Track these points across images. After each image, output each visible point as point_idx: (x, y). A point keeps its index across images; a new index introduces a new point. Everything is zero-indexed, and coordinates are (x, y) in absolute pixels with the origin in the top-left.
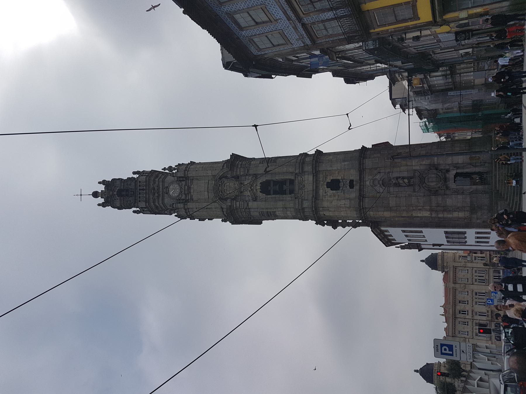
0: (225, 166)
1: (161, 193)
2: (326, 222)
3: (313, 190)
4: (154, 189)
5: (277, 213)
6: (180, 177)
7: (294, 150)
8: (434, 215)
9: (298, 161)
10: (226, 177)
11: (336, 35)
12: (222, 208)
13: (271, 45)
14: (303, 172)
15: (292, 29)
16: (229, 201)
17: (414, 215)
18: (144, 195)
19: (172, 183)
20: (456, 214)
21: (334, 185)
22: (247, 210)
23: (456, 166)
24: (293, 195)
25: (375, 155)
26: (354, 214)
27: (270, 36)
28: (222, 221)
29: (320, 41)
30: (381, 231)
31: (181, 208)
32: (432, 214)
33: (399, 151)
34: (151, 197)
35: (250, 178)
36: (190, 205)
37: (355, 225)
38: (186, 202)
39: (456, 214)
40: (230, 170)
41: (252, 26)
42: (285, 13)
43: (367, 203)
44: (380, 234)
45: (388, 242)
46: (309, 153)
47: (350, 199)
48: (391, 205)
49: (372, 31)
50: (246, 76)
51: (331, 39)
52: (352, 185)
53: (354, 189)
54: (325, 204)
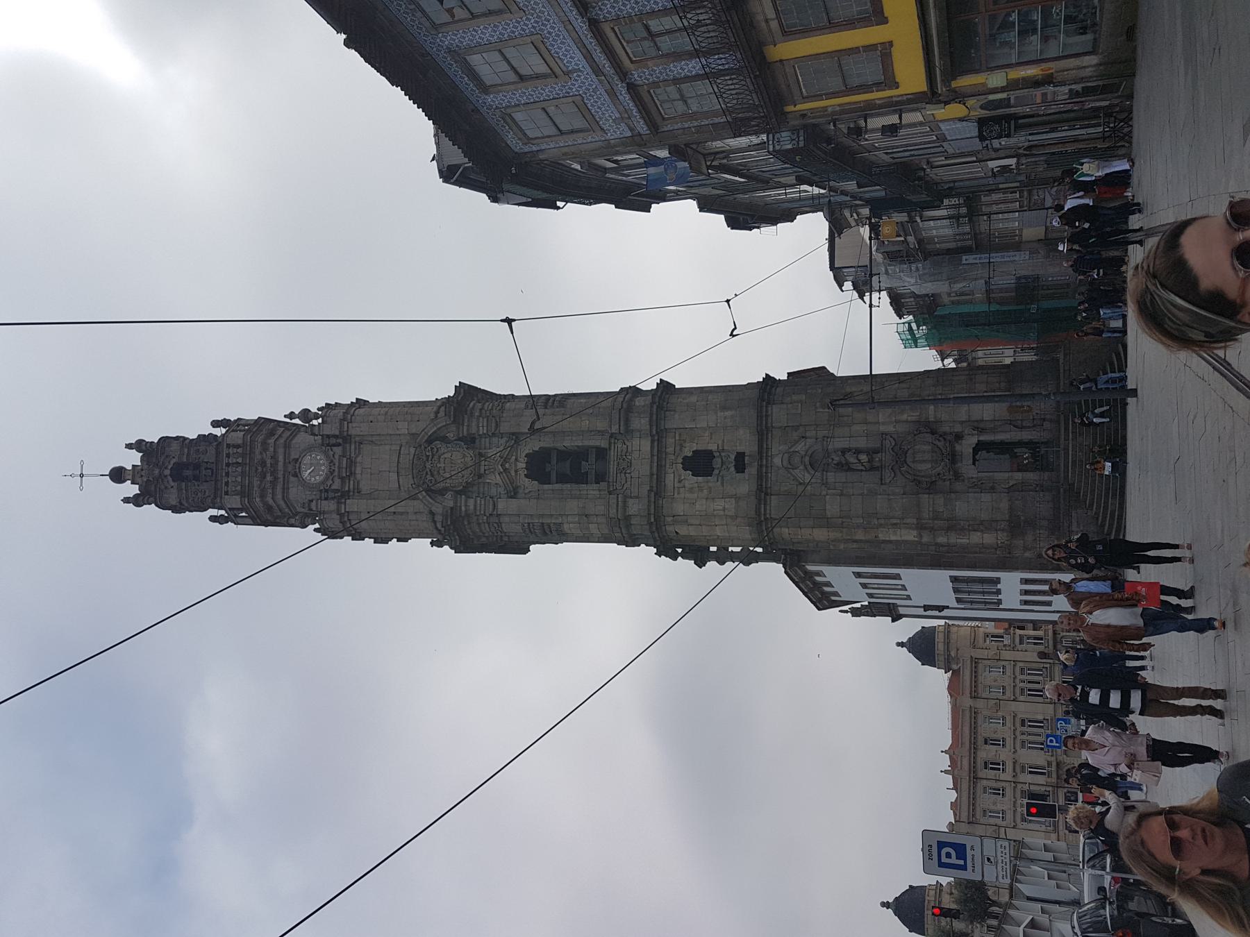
0: (442, 413)
1: (280, 475)
2: (680, 550)
3: (652, 474)
4: (263, 463)
5: (566, 526)
6: (328, 436)
7: (607, 378)
8: (925, 539)
9: (618, 405)
11: (706, 115)
12: (432, 513)
13: (553, 131)
14: (628, 432)
16: (449, 495)
17: (881, 537)
18: (239, 479)
19: (310, 449)
20: (976, 538)
21: (701, 464)
22: (492, 520)
23: (979, 427)
24: (604, 485)
25: (795, 397)
26: (746, 533)
27: (551, 110)
28: (432, 544)
29: (669, 127)
30: (806, 572)
31: (330, 512)
32: (921, 536)
33: (848, 390)
34: (256, 483)
35: (503, 441)
36: (352, 505)
38: (343, 496)
39: (976, 538)
40: (454, 422)
41: (509, 84)
42: (588, 56)
43: (775, 506)
44: (803, 580)
45: (822, 598)
46: (644, 387)
47: (737, 498)
48: (829, 514)
49: (790, 108)
50: (494, 199)
53: (746, 475)
54: (680, 508)
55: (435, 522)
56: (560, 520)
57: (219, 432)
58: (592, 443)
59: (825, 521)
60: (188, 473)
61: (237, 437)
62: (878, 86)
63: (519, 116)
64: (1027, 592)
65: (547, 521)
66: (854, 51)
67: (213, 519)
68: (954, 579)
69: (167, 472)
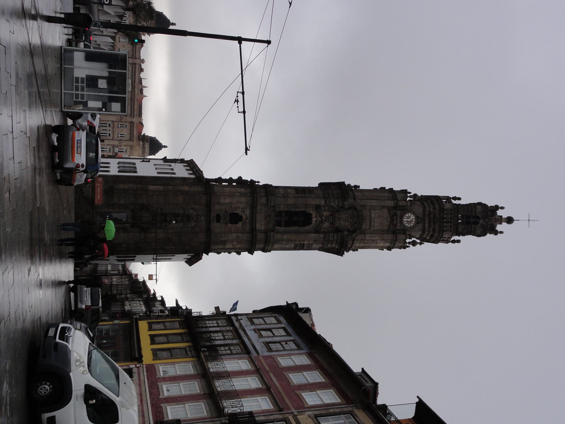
1: (427, 218)
3: (256, 214)
4: (434, 223)
5: (294, 192)
7: (277, 257)
10: (349, 231)
12: (355, 199)
14: (266, 232)
16: (347, 206)
17: (162, 187)
18: (445, 216)
21: (235, 218)
24: (277, 210)
28: (359, 187)
35: (322, 230)
36: (391, 203)
37: (220, 180)
38: (396, 207)
39: (126, 187)
45: (191, 165)
54: (243, 199)
55: (354, 195)
56: (297, 195)
57: (456, 238)
58: (283, 228)
62: (154, 323)
64: (108, 167)
67: (459, 199)
68: (136, 172)
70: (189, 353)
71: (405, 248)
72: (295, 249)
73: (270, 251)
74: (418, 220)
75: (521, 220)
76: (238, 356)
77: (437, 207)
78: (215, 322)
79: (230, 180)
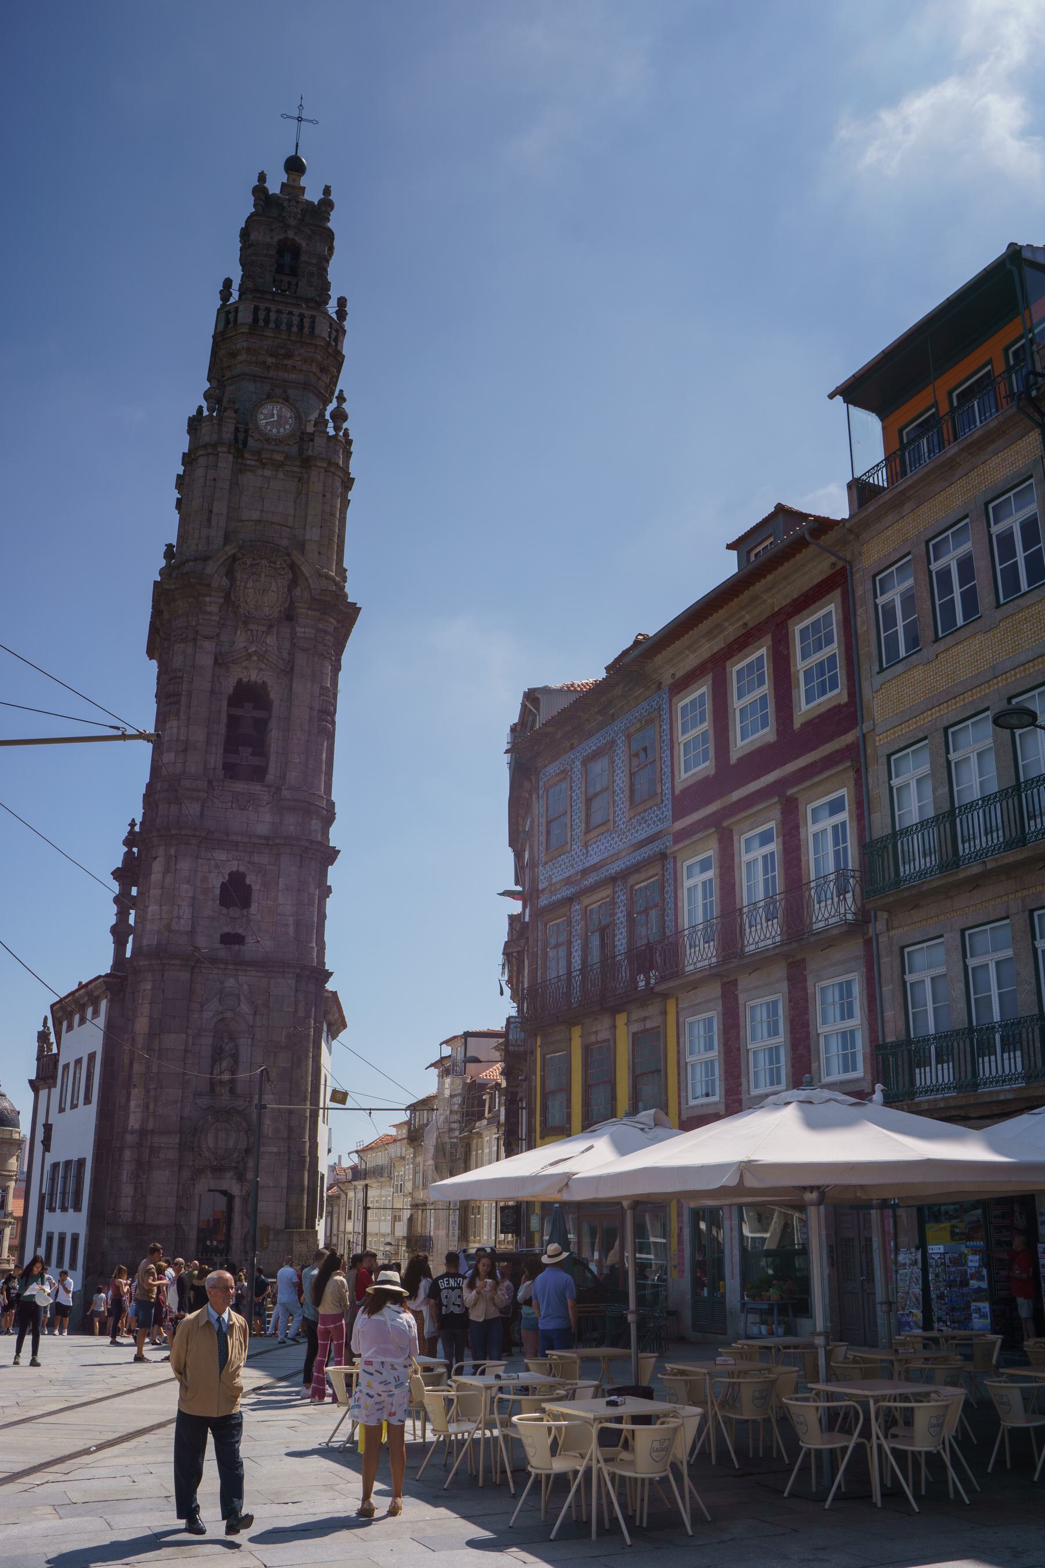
4: (289, 355)
5: (174, 723)
6: (312, 440)
8: (129, 1138)
10: (293, 583)
12: (206, 559)
15: (567, 875)
16: (225, 582)
19: (298, 417)
20: (127, 1190)
23: (252, 1197)
24: (220, 773)
28: (170, 546)
29: (540, 927)
35: (285, 655)
36: (226, 462)
37: (119, 933)
39: (127, 1190)
42: (594, 868)
44: (89, 994)
46: (333, 830)
47: (192, 933)
51: (540, 952)
52: (232, 939)
53: (218, 946)
54: (185, 865)
55: (196, 560)
56: (183, 717)
57: (332, 308)
58: (272, 765)
59: (157, 1029)
60: (288, 258)
61: (323, 330)
62: (544, 1122)
63: (564, 785)
65: (184, 700)
66: (569, 1106)
67: (228, 283)
68: (81, 1162)
69: (291, 234)
70: (649, 1025)
71: (350, 442)
72: (331, 736)
73: (333, 804)
74: (278, 393)
75: (298, 139)
76: (669, 889)
77: (245, 344)
78: (552, 954)
79: (123, 902)
